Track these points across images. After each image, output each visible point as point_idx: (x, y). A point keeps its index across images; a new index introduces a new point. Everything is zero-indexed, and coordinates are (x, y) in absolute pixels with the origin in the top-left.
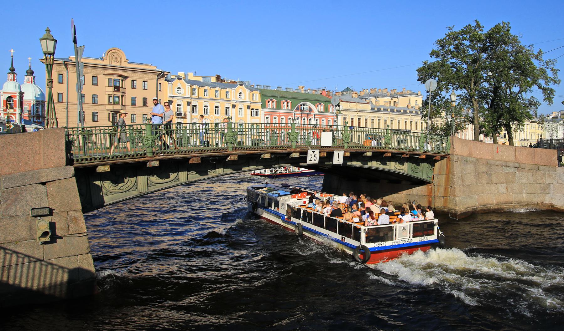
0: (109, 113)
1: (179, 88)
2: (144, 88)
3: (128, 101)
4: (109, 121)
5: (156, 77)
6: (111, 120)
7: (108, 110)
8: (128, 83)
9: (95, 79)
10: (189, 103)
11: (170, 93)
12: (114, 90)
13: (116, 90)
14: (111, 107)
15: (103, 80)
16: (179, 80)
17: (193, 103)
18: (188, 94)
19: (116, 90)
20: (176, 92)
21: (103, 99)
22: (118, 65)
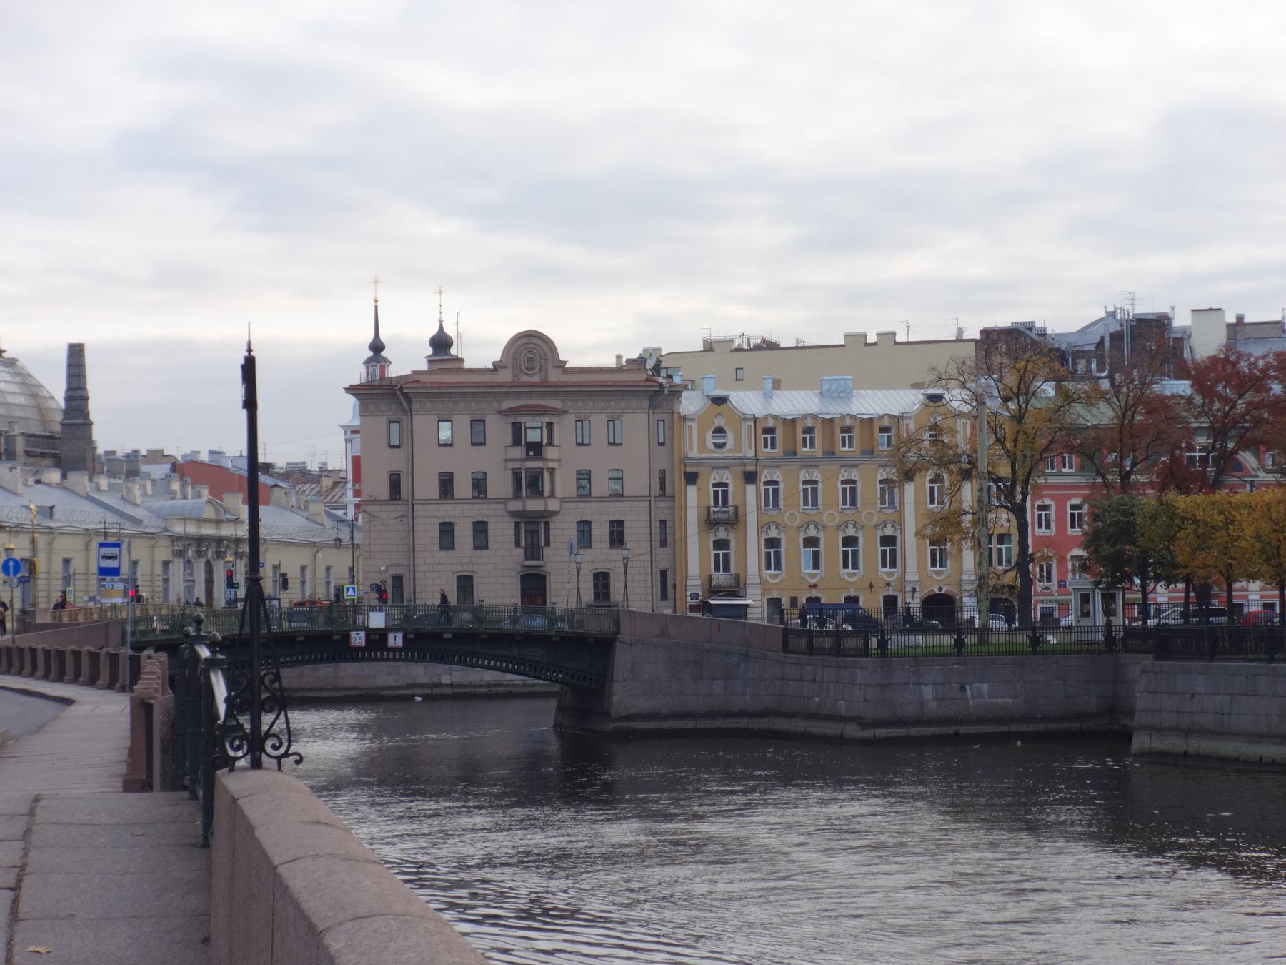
0: (517, 525)
1: (720, 430)
2: (611, 441)
3: (565, 484)
4: (518, 544)
5: (646, 404)
6: (523, 544)
7: (513, 514)
8: (565, 430)
9: (479, 427)
10: (751, 477)
11: (691, 448)
12: (527, 454)
13: (531, 453)
14: (516, 506)
15: (498, 431)
16: (719, 405)
17: (765, 476)
18: (750, 448)
19: (531, 453)
20: (710, 441)
21: (499, 485)
22: (536, 379)
